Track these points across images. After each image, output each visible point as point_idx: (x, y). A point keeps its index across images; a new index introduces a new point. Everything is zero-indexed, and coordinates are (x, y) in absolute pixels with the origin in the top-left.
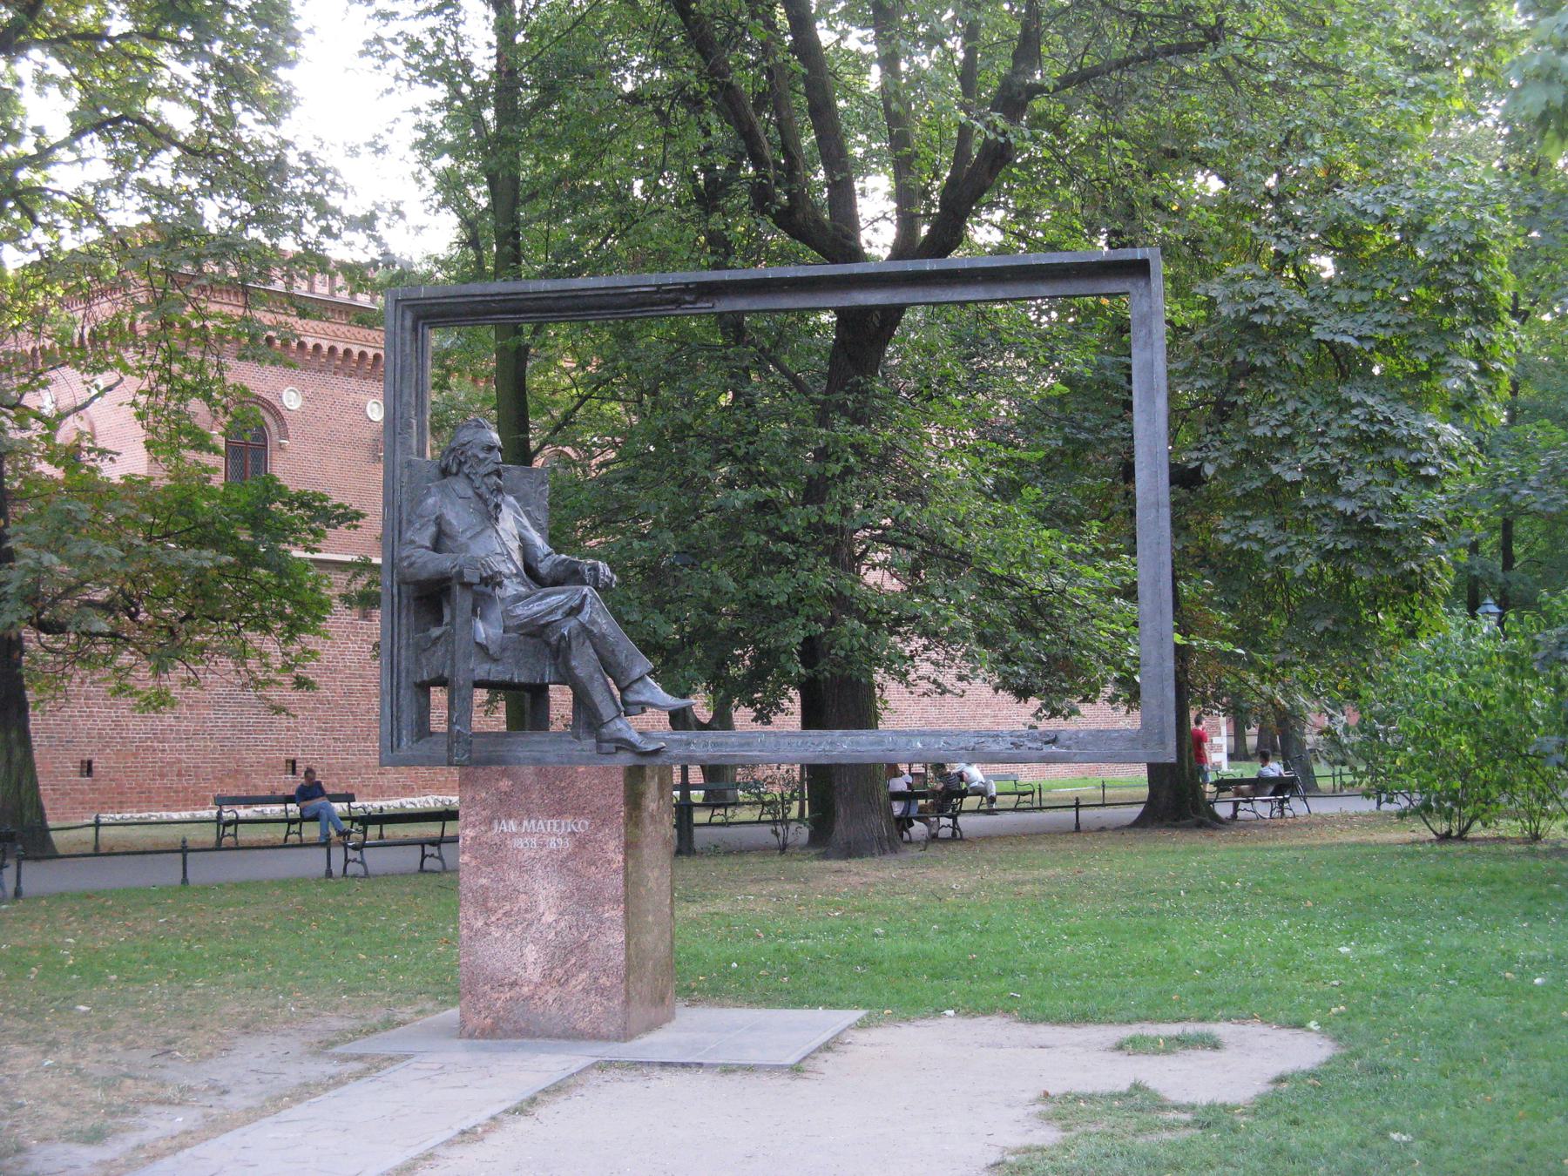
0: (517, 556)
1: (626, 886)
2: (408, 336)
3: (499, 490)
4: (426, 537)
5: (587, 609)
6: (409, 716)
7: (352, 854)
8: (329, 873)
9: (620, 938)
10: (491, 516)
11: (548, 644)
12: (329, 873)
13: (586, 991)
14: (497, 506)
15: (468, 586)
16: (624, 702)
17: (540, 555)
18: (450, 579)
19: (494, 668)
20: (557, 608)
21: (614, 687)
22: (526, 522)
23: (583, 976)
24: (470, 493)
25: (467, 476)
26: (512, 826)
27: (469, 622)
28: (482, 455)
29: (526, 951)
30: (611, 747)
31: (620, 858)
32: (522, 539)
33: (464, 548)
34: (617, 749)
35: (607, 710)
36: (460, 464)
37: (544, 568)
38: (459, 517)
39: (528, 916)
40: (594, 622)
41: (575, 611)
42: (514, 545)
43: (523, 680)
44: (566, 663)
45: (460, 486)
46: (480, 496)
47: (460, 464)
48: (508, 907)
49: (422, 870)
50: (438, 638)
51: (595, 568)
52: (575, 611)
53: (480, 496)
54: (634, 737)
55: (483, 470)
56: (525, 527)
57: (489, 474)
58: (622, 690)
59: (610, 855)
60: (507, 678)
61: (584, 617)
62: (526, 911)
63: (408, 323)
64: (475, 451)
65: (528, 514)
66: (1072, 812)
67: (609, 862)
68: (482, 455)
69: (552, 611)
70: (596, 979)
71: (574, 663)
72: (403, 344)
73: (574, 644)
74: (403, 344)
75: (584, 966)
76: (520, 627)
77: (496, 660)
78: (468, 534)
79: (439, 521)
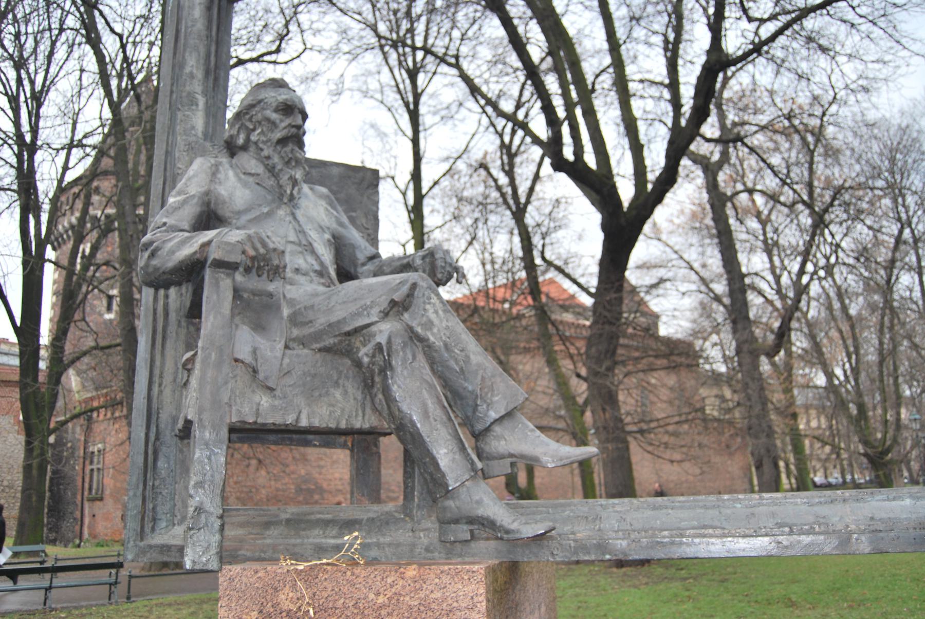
0: (327, 255)
19: (265, 401)
24: (260, 169)
28: (274, 116)
43: (316, 423)
55: (278, 135)
56: (341, 224)
58: (478, 436)
60: (290, 420)
68: (274, 116)
76: (317, 336)
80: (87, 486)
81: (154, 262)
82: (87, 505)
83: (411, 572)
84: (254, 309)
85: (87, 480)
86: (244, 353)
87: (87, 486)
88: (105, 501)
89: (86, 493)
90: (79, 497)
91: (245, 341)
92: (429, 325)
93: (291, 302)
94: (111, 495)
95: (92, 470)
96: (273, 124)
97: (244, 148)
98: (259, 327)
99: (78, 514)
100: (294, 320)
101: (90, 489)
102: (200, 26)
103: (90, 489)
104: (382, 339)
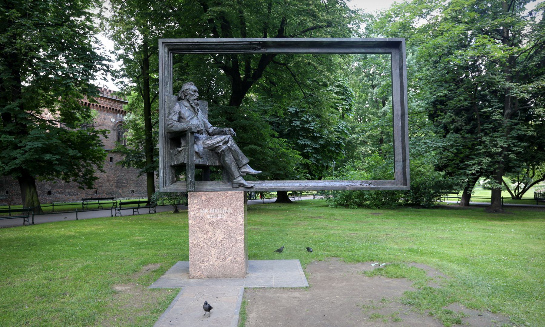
2: (166, 55)
4: (176, 118)
5: (230, 142)
7: (117, 211)
8: (112, 216)
11: (217, 153)
12: (112, 216)
13: (232, 263)
15: (193, 133)
18: (186, 131)
19: (200, 160)
20: (220, 141)
23: (230, 258)
24: (188, 105)
25: (188, 100)
26: (206, 211)
27: (193, 145)
29: (212, 250)
31: (243, 220)
34: (239, 186)
36: (185, 96)
38: (186, 112)
39: (212, 239)
40: (232, 146)
41: (226, 143)
44: (224, 159)
46: (192, 106)
47: (185, 96)
48: (205, 237)
49: (133, 215)
50: (181, 151)
51: (230, 130)
52: (226, 143)
53: (192, 106)
55: (193, 98)
57: (195, 100)
59: (239, 220)
61: (229, 145)
62: (212, 238)
63: (166, 51)
64: (190, 92)
67: (239, 222)
68: (192, 93)
69: (218, 143)
70: (235, 258)
71: (226, 159)
72: (165, 57)
73: (226, 153)
74: (165, 57)
75: (231, 255)
76: (209, 147)
77: (201, 158)
78: (190, 118)
79: (180, 113)
81: (172, 128)
83: (230, 192)
96: (192, 95)
104: (224, 149)
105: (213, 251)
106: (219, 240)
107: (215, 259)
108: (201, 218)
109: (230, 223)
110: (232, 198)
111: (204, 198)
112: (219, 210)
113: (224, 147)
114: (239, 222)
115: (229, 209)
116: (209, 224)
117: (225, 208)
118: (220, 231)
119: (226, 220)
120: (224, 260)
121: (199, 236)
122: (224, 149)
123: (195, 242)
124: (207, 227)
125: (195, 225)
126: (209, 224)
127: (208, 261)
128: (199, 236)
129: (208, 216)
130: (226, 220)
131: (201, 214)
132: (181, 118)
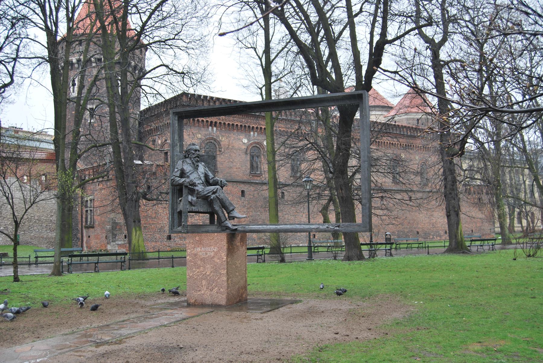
1: (227, 265)
3: (198, 161)
4: (178, 174)
6: (176, 221)
9: (225, 279)
10: (196, 168)
13: (217, 293)
14: (198, 166)
15: (186, 187)
16: (229, 217)
17: (210, 178)
21: (225, 212)
22: (207, 169)
23: (216, 289)
24: (191, 162)
26: (199, 249)
30: (224, 228)
32: (206, 174)
33: (188, 177)
34: (227, 229)
35: (223, 219)
37: (211, 181)
38: (188, 168)
41: (214, 193)
42: (202, 176)
45: (188, 160)
46: (193, 163)
53: (193, 163)
54: (230, 226)
55: (194, 156)
57: (195, 157)
58: (228, 213)
63: (176, 118)
65: (208, 168)
66: (157, 253)
67: (223, 258)
69: (208, 193)
75: (217, 286)
76: (202, 196)
77: (194, 206)
80: (84, 220)
82: (84, 231)
83: (216, 234)
84: (192, 192)
85: (84, 216)
86: (190, 200)
87: (84, 220)
88: (95, 228)
89: (84, 224)
90: (80, 226)
91: (190, 198)
92: (220, 196)
93: (197, 190)
94: (99, 225)
95: (87, 211)
96: (194, 154)
97: (188, 157)
98: (192, 195)
99: (79, 235)
100: (197, 194)
101: (86, 221)
102: (177, 128)
103: (86, 221)
104: (212, 198)
105: (204, 282)
106: (208, 273)
107: (205, 289)
108: (195, 255)
109: (216, 259)
110: (218, 239)
111: (197, 238)
112: (208, 249)
113: (213, 196)
114: (223, 258)
115: (216, 248)
116: (201, 259)
117: (213, 247)
118: (208, 266)
119: (213, 257)
120: (211, 290)
121: (194, 269)
122: (212, 198)
123: (191, 275)
124: (199, 262)
125: (191, 261)
126: (201, 259)
127: (200, 290)
128: (194, 269)
129: (200, 254)
130: (213, 257)
131: (195, 252)
132: (183, 174)
